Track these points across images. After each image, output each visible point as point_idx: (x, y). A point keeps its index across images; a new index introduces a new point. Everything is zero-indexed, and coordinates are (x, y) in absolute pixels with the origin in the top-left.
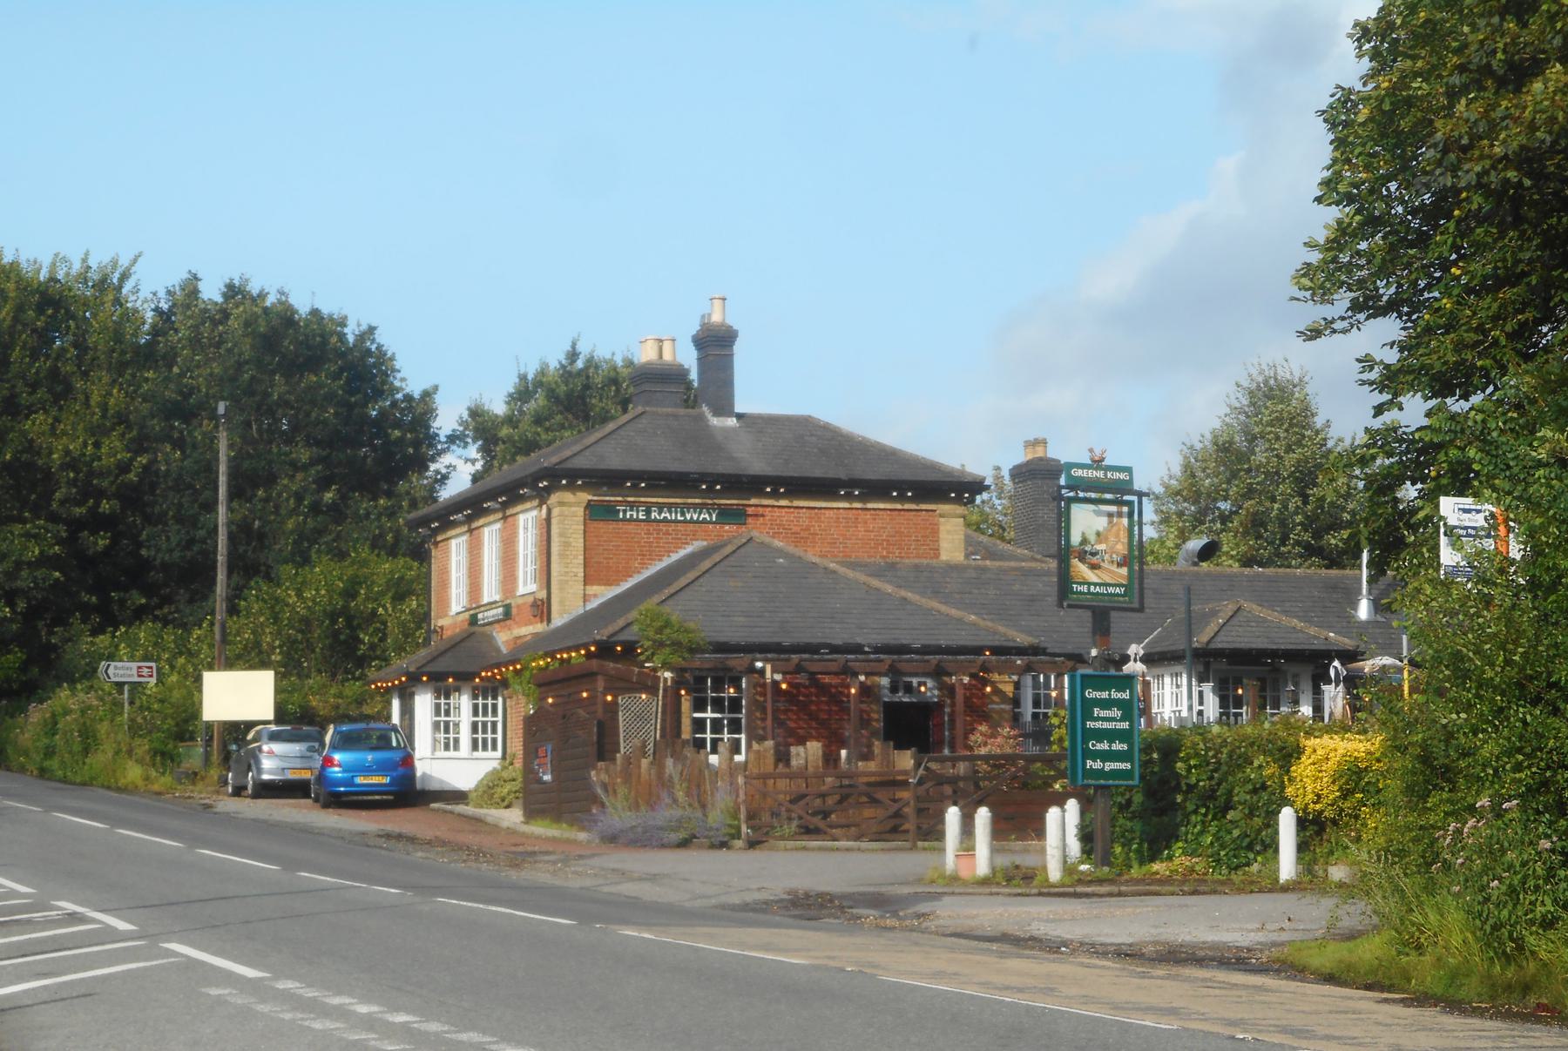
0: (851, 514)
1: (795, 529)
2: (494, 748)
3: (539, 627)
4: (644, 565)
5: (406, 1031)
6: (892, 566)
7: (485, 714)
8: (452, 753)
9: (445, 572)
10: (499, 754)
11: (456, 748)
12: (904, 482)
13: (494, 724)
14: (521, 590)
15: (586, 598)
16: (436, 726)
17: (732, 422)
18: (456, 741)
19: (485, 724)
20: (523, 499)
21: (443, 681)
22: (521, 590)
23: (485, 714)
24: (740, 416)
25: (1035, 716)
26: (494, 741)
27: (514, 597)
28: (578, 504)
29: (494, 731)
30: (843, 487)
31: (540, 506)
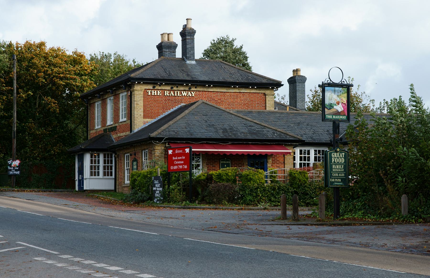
0: (235, 94)
1: (216, 99)
2: (111, 175)
3: (128, 133)
4: (164, 112)
5: (116, 273)
6: (251, 112)
7: (95, 163)
8: (97, 177)
9: (94, 114)
10: (113, 177)
11: (98, 175)
12: (253, 83)
13: (111, 167)
14: (121, 120)
15: (144, 123)
16: (91, 167)
17: (194, 62)
18: (98, 172)
19: (95, 167)
20: (120, 88)
21: (94, 150)
22: (121, 120)
23: (95, 163)
24: (196, 60)
25: (300, 164)
26: (111, 172)
27: (118, 123)
28: (141, 90)
29: (111, 169)
30: (232, 85)
31: (128, 91)
